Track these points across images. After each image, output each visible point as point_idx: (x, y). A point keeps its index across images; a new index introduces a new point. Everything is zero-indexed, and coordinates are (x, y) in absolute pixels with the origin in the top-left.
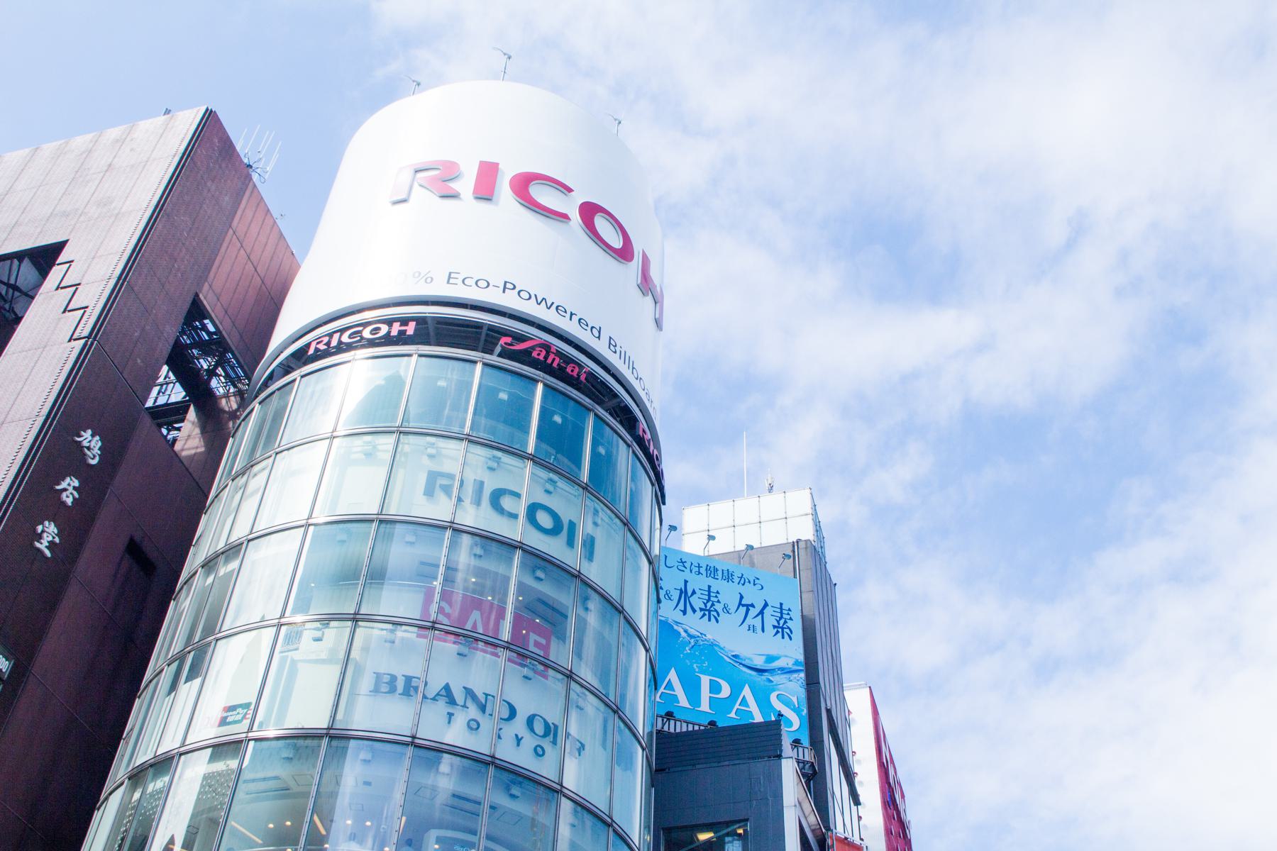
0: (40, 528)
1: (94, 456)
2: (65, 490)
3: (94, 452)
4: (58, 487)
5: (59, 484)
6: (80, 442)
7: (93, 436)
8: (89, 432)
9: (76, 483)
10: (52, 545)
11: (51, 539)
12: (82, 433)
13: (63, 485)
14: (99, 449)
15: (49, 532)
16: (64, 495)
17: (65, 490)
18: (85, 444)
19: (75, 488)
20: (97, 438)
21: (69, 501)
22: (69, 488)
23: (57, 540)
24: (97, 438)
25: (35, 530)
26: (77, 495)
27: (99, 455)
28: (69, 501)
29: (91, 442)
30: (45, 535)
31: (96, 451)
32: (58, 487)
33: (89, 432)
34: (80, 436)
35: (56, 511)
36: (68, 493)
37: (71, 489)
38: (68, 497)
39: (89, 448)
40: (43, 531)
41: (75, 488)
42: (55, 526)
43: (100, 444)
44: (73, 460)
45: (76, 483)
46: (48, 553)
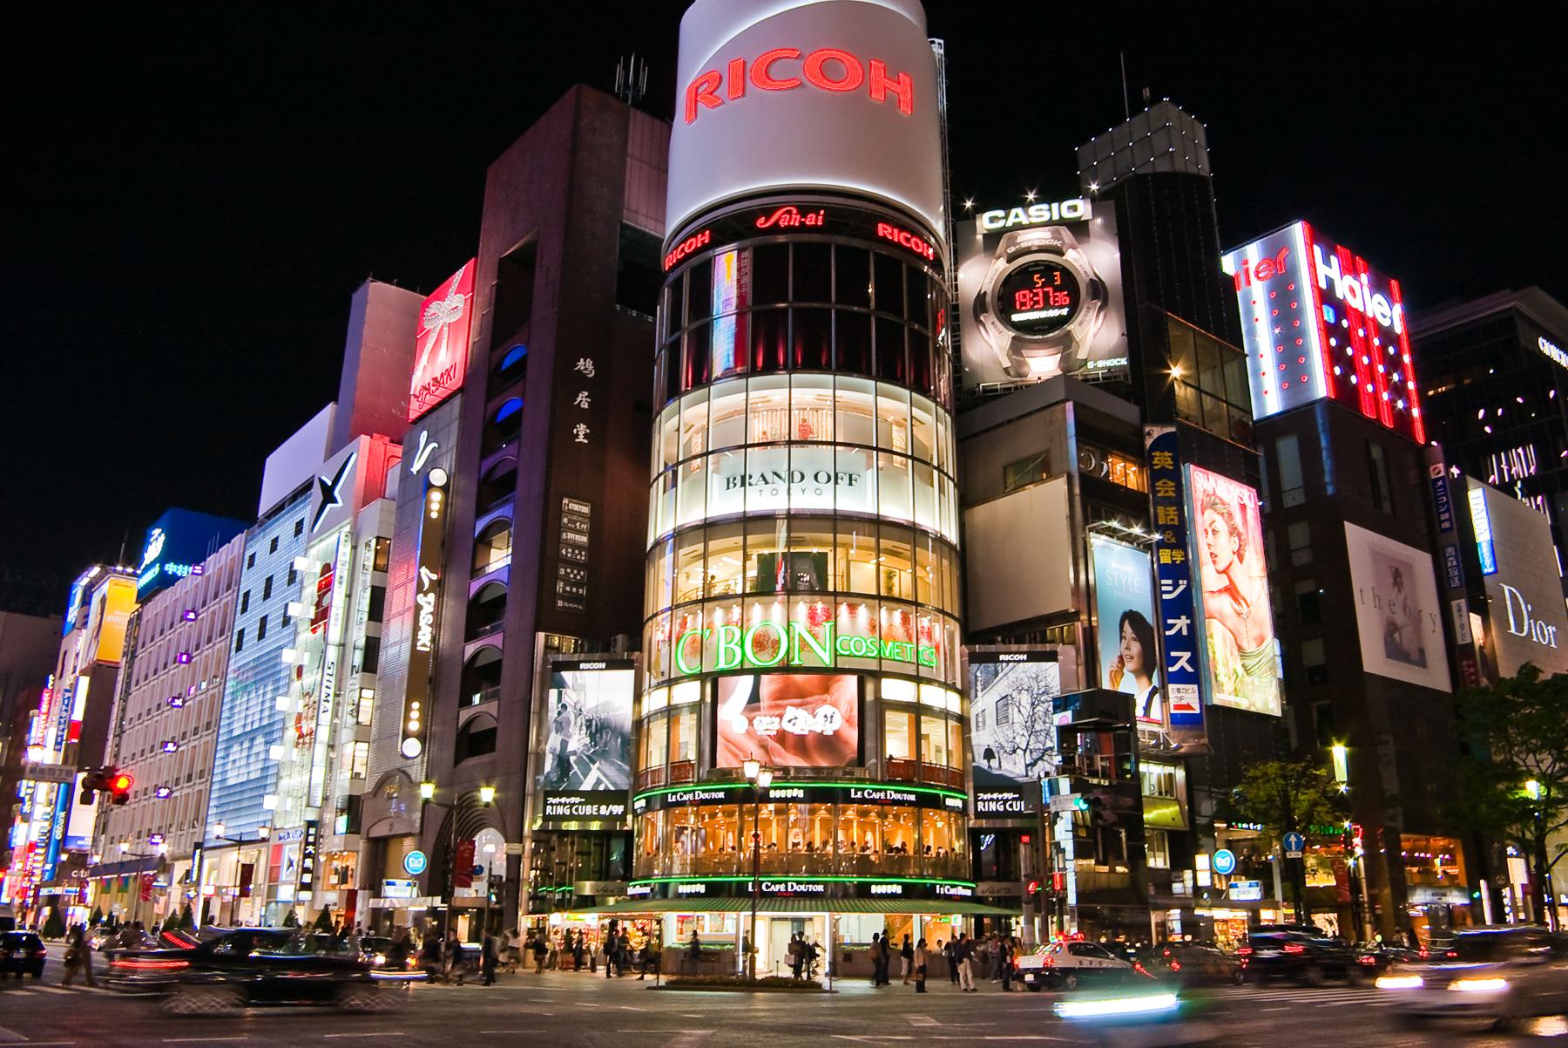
0: (575, 431)
7: (585, 361)
9: (586, 394)
10: (586, 436)
13: (579, 399)
15: (582, 429)
18: (582, 368)
21: (586, 406)
22: (583, 400)
28: (586, 406)
29: (586, 366)
31: (591, 367)
35: (582, 416)
37: (584, 399)
39: (586, 369)
44: (581, 382)
45: (586, 394)
46: (586, 441)
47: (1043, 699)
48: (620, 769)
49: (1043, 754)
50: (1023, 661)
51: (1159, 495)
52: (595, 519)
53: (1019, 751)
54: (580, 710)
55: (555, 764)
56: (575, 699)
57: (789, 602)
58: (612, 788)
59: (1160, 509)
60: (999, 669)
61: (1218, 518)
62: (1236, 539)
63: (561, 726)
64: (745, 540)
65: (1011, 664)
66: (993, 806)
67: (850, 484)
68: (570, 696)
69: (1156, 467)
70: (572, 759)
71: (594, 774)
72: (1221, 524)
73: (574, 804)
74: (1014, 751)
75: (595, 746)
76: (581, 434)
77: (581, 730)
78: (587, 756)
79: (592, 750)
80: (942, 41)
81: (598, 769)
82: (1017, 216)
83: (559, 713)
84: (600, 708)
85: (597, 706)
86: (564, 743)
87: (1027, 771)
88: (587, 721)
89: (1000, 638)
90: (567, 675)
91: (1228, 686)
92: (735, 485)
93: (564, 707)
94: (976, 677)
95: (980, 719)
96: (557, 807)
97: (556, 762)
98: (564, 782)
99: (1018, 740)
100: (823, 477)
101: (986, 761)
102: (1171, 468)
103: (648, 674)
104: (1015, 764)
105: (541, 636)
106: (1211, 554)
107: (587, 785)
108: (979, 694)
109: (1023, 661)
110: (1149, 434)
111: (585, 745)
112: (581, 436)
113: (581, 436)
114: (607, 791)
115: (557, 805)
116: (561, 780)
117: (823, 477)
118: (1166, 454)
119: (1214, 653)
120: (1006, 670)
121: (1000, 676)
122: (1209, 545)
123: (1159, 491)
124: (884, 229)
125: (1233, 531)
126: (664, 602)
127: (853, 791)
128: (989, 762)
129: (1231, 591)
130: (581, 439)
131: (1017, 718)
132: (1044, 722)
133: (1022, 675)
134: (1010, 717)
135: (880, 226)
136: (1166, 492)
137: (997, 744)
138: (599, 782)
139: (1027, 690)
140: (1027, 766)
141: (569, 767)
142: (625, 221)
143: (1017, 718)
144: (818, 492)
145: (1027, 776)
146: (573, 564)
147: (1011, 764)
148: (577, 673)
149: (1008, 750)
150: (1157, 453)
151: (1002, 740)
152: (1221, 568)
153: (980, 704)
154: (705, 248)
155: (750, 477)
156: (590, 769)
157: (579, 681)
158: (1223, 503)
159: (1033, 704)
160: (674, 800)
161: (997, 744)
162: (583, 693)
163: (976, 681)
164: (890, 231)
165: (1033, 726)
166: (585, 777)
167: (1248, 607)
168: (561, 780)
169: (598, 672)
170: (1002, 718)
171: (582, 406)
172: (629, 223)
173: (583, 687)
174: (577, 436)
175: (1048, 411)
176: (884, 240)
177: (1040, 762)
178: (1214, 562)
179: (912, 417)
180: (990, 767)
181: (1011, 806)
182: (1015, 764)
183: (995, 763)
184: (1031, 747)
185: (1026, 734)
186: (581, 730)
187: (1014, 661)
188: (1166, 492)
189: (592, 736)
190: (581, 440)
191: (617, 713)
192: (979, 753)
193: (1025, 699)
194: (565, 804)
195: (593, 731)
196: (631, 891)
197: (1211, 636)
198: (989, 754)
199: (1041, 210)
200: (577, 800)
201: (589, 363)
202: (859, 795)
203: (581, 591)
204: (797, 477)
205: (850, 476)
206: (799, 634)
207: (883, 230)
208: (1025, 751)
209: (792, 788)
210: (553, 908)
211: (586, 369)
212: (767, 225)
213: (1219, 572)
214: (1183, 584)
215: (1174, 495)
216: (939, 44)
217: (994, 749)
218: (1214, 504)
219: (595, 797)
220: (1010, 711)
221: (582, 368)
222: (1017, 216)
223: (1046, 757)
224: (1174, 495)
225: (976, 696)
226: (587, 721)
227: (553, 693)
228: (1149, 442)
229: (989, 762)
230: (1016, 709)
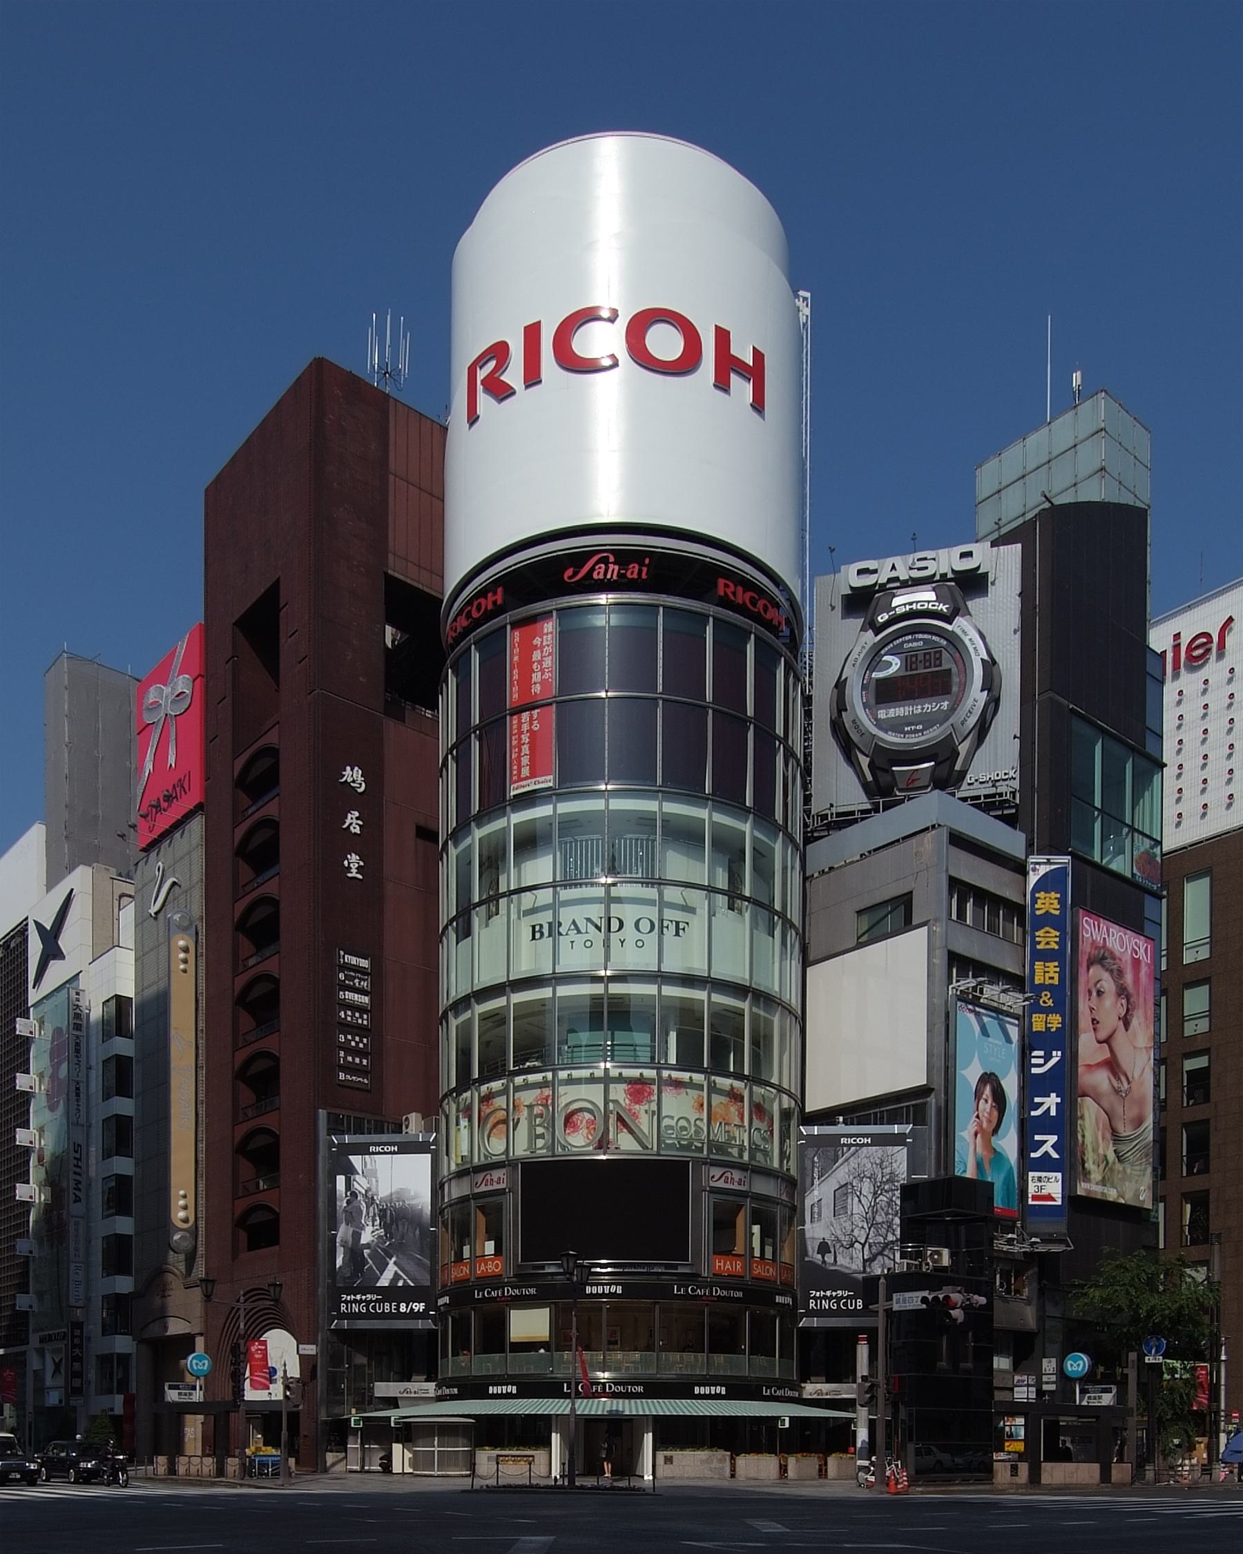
0: (346, 863)
1: (361, 784)
2: (351, 824)
3: (359, 782)
4: (345, 826)
7: (352, 770)
8: (348, 768)
10: (359, 869)
11: (357, 865)
12: (344, 773)
13: (348, 821)
14: (362, 776)
15: (354, 860)
16: (351, 828)
17: (351, 824)
19: (357, 818)
20: (356, 768)
21: (358, 830)
22: (353, 822)
23: (362, 864)
24: (356, 768)
25: (343, 865)
26: (361, 823)
28: (358, 830)
29: (353, 775)
31: (360, 779)
32: (345, 826)
33: (348, 768)
36: (354, 825)
37: (355, 821)
38: (354, 828)
39: (354, 781)
40: (349, 863)
41: (357, 818)
42: (356, 854)
43: (360, 772)
45: (357, 814)
47: (887, 1187)
48: (419, 1263)
49: (884, 1249)
50: (867, 1145)
51: (1038, 947)
53: (857, 1245)
54: (373, 1198)
55: (347, 1258)
56: (366, 1186)
58: (412, 1285)
59: (1039, 965)
60: (840, 1152)
61: (1106, 976)
62: (1124, 1001)
63: (353, 1217)
65: (853, 1148)
66: (825, 1304)
68: (360, 1184)
69: (1038, 913)
70: (366, 1252)
71: (391, 1269)
72: (1108, 984)
73: (371, 1301)
74: (852, 1245)
75: (391, 1238)
76: (354, 867)
77: (374, 1221)
78: (382, 1250)
79: (388, 1243)
80: (808, 295)
81: (395, 1263)
82: (893, 567)
83: (348, 1202)
84: (393, 1196)
85: (391, 1194)
86: (357, 1236)
87: (864, 1267)
88: (380, 1210)
89: (841, 1119)
90: (356, 1160)
91: (1096, 1175)
93: (354, 1195)
94: (813, 1162)
95: (816, 1210)
96: (353, 1303)
97: (348, 1255)
98: (358, 1278)
99: (856, 1233)
101: (819, 1256)
102: (1057, 913)
103: (446, 1157)
104: (852, 1258)
105: (322, 1113)
106: (1093, 1020)
107: (384, 1282)
108: (816, 1182)
109: (867, 1145)
110: (1034, 870)
111: (380, 1237)
112: (354, 871)
114: (406, 1286)
115: (351, 1302)
116: (354, 1276)
118: (1053, 895)
119: (1083, 1136)
120: (846, 1155)
121: (840, 1161)
122: (1092, 1009)
123: (1039, 943)
125: (1122, 992)
128: (823, 1257)
129: (1112, 1065)
130: (354, 873)
131: (857, 1208)
132: (887, 1214)
133: (866, 1161)
134: (849, 1207)
136: (1048, 943)
137: (833, 1238)
138: (397, 1277)
139: (870, 1178)
140: (865, 1261)
141: (364, 1262)
142: (390, 572)
143: (857, 1208)
144: (640, 944)
145: (864, 1271)
147: (848, 1260)
148: (367, 1156)
149: (845, 1243)
150: (1042, 895)
151: (839, 1232)
152: (1103, 1035)
153: (816, 1193)
156: (388, 1264)
157: (369, 1166)
158: (1114, 957)
159: (875, 1193)
161: (833, 1238)
162: (374, 1180)
163: (813, 1167)
164: (733, 589)
165: (874, 1218)
166: (381, 1274)
167: (1129, 1083)
168: (354, 1276)
169: (390, 1156)
170: (840, 1207)
171: (353, 831)
172: (396, 575)
173: (374, 1173)
174: (349, 868)
175: (914, 840)
177: (880, 1258)
178: (1095, 1030)
180: (824, 1262)
181: (845, 1304)
182: (852, 1258)
183: (829, 1258)
184: (871, 1241)
185: (865, 1226)
186: (374, 1221)
187: (857, 1145)
188: (1048, 943)
189: (384, 1225)
190: (354, 875)
191: (414, 1202)
192: (812, 1248)
193: (867, 1187)
194: (361, 1301)
195: (388, 1222)
197: (1082, 1117)
198: (824, 1248)
199: (919, 569)
200: (375, 1297)
203: (365, 1062)
208: (863, 1245)
211: (354, 781)
212: (573, 580)
213: (1099, 1042)
214: (1056, 1056)
215: (1056, 947)
216: (805, 299)
217: (829, 1243)
218: (1104, 958)
219: (391, 1293)
220: (849, 1200)
222: (893, 567)
223: (886, 1253)
224: (1056, 947)
225: (813, 1184)
226: (380, 1210)
227: (341, 1180)
228: (1033, 879)
229: (823, 1257)
230: (856, 1199)
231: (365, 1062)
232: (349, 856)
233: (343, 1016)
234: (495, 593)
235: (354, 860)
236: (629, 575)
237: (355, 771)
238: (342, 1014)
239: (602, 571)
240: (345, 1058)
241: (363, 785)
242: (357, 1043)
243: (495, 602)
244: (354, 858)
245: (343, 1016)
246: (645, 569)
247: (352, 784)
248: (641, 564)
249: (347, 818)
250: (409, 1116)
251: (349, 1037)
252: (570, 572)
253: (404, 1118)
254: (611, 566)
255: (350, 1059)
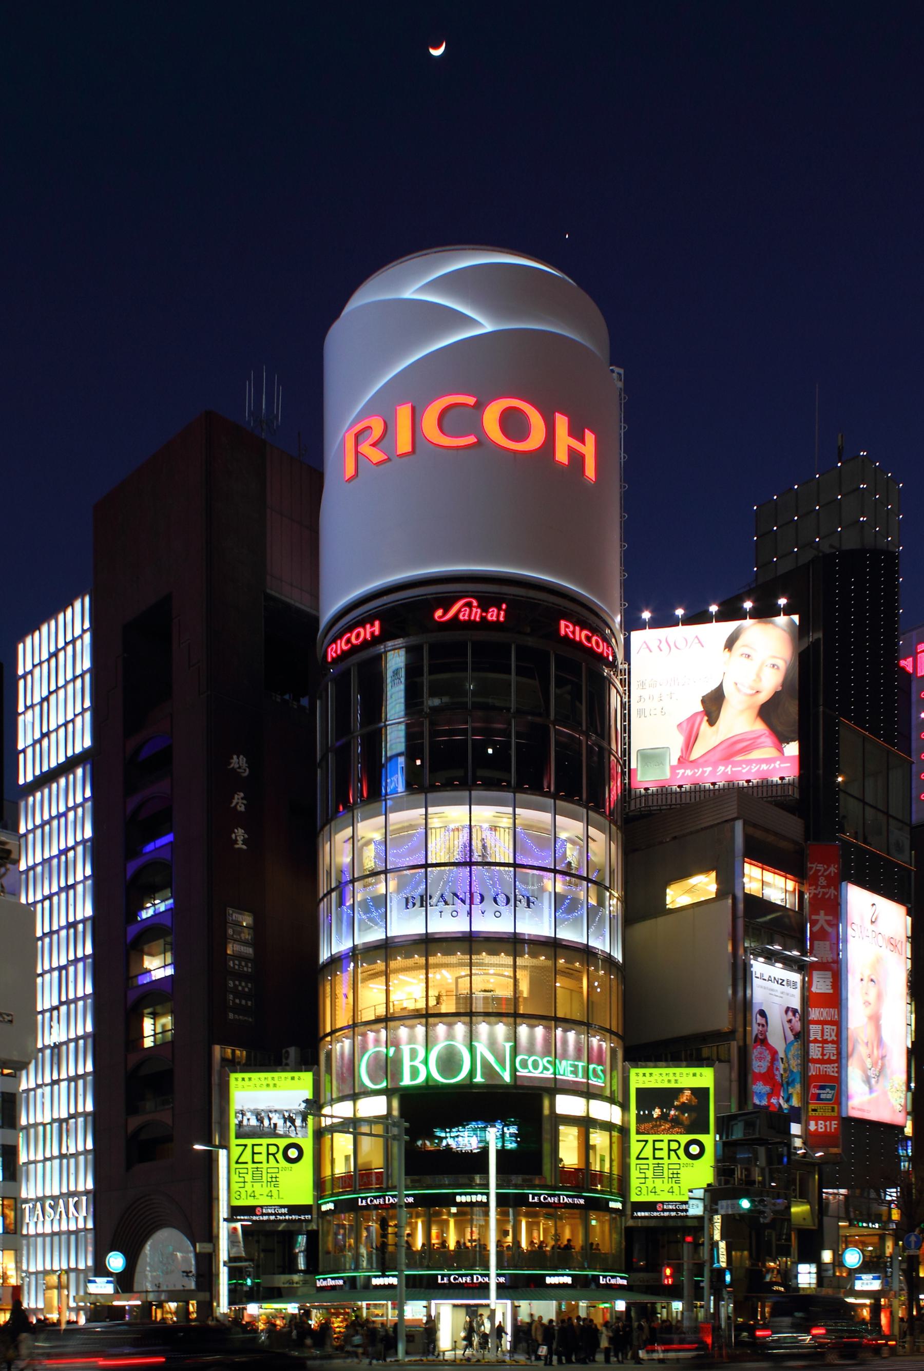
0: (233, 836)
1: (245, 770)
3: (244, 767)
4: (233, 805)
5: (231, 803)
6: (233, 768)
7: (238, 758)
8: (235, 757)
9: (242, 795)
10: (245, 842)
13: (235, 801)
14: (247, 762)
15: (240, 834)
16: (238, 807)
17: (237, 803)
18: (236, 766)
22: (239, 801)
23: (246, 836)
26: (245, 802)
27: (248, 767)
28: (241, 808)
30: (238, 838)
31: (245, 765)
32: (233, 805)
33: (235, 757)
34: (231, 763)
36: (240, 804)
37: (240, 801)
39: (239, 768)
40: (236, 836)
43: (245, 759)
45: (242, 795)
46: (244, 847)
52: (256, 928)
57: (471, 1023)
64: (427, 960)
67: (529, 906)
76: (240, 839)
92: (414, 904)
100: (501, 899)
112: (240, 842)
113: (240, 842)
117: (501, 899)
124: (567, 626)
126: (343, 1019)
127: (531, 1196)
135: (563, 623)
146: (240, 976)
154: (376, 640)
155: (431, 897)
160: (364, 1203)
174: (236, 840)
176: (568, 641)
179: (588, 837)
196: (319, 1284)
201: (243, 760)
202: (536, 1200)
204: (477, 899)
205: (528, 898)
206: (481, 1053)
207: (565, 628)
209: (476, 1194)
210: (244, 1299)
221: (236, 766)
231: (249, 1003)
232: (236, 831)
233: (232, 965)
234: (372, 625)
235: (240, 834)
236: (489, 617)
237: (240, 759)
238: (231, 964)
239: (467, 613)
240: (234, 1001)
241: (247, 770)
242: (243, 988)
243: (372, 633)
244: (240, 831)
245: (232, 965)
246: (502, 613)
247: (238, 770)
248: (499, 609)
249: (233, 798)
250: (288, 1049)
251: (237, 983)
252: (439, 613)
253: (284, 1051)
254: (474, 610)
255: (237, 1001)
